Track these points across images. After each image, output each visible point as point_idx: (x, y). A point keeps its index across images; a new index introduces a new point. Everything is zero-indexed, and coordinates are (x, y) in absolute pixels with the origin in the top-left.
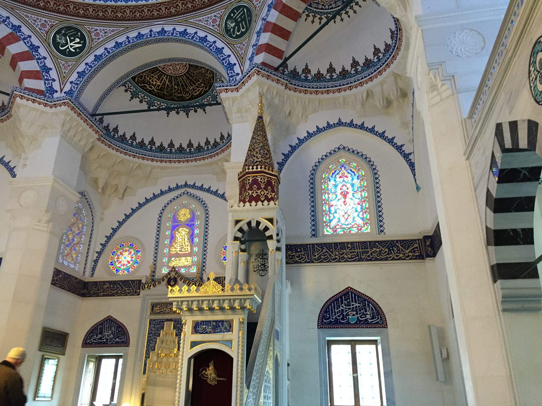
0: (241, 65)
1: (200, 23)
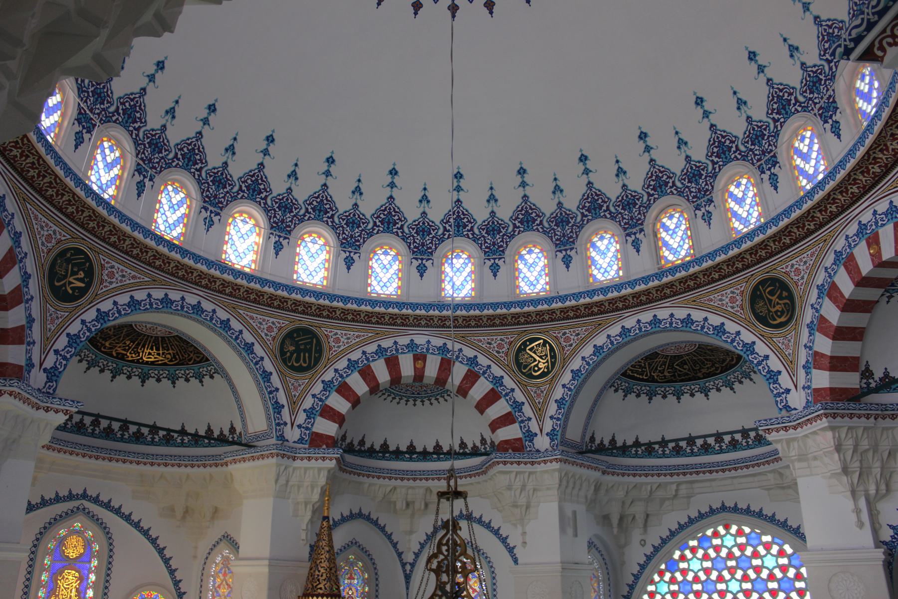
0: (293, 413)
1: (251, 321)
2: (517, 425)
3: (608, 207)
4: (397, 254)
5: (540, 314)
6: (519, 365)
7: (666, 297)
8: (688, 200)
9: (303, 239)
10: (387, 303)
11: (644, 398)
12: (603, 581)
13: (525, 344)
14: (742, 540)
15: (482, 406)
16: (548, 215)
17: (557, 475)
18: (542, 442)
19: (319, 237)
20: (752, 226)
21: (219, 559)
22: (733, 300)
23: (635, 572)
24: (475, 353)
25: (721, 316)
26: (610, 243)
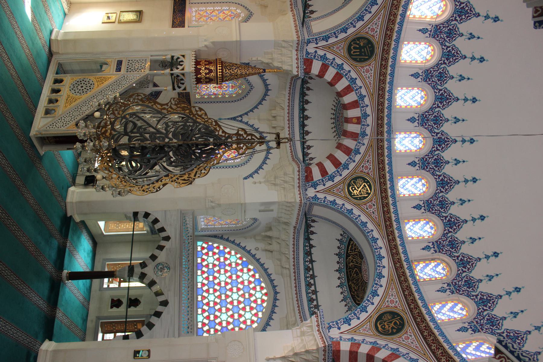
0: (324, 48)
1: (377, 18)
2: (320, 178)
3: (451, 232)
4: (422, 105)
5: (386, 191)
6: (356, 179)
7: (395, 264)
8: (454, 280)
9: (429, 46)
10: (390, 100)
11: (337, 251)
12: (236, 227)
13: (368, 182)
14: (259, 302)
15: (332, 158)
16: (446, 196)
17: (293, 200)
18: (311, 192)
19: (431, 56)
20: (436, 315)
21: (239, 11)
22: (392, 302)
23: (241, 245)
24: (362, 153)
25: (382, 294)
26: (429, 233)
